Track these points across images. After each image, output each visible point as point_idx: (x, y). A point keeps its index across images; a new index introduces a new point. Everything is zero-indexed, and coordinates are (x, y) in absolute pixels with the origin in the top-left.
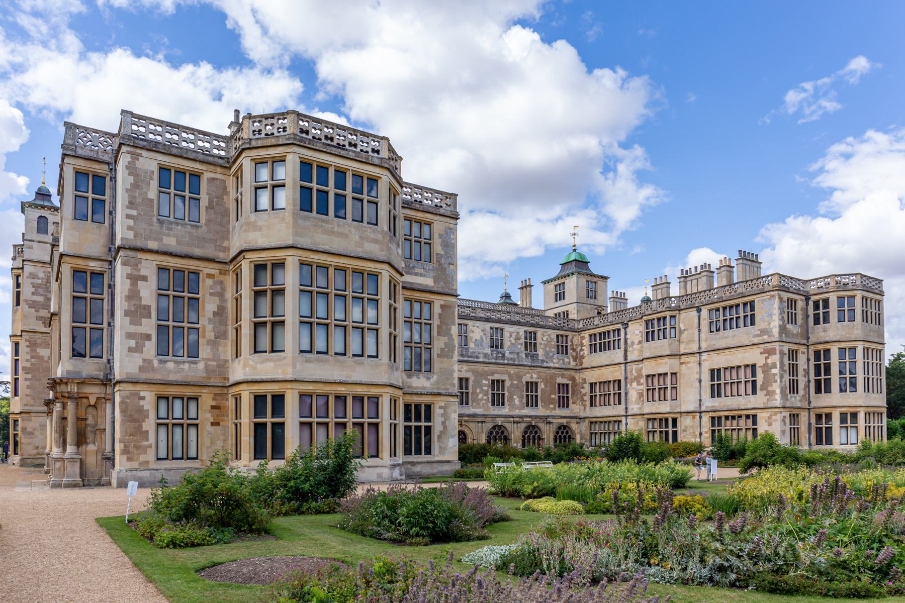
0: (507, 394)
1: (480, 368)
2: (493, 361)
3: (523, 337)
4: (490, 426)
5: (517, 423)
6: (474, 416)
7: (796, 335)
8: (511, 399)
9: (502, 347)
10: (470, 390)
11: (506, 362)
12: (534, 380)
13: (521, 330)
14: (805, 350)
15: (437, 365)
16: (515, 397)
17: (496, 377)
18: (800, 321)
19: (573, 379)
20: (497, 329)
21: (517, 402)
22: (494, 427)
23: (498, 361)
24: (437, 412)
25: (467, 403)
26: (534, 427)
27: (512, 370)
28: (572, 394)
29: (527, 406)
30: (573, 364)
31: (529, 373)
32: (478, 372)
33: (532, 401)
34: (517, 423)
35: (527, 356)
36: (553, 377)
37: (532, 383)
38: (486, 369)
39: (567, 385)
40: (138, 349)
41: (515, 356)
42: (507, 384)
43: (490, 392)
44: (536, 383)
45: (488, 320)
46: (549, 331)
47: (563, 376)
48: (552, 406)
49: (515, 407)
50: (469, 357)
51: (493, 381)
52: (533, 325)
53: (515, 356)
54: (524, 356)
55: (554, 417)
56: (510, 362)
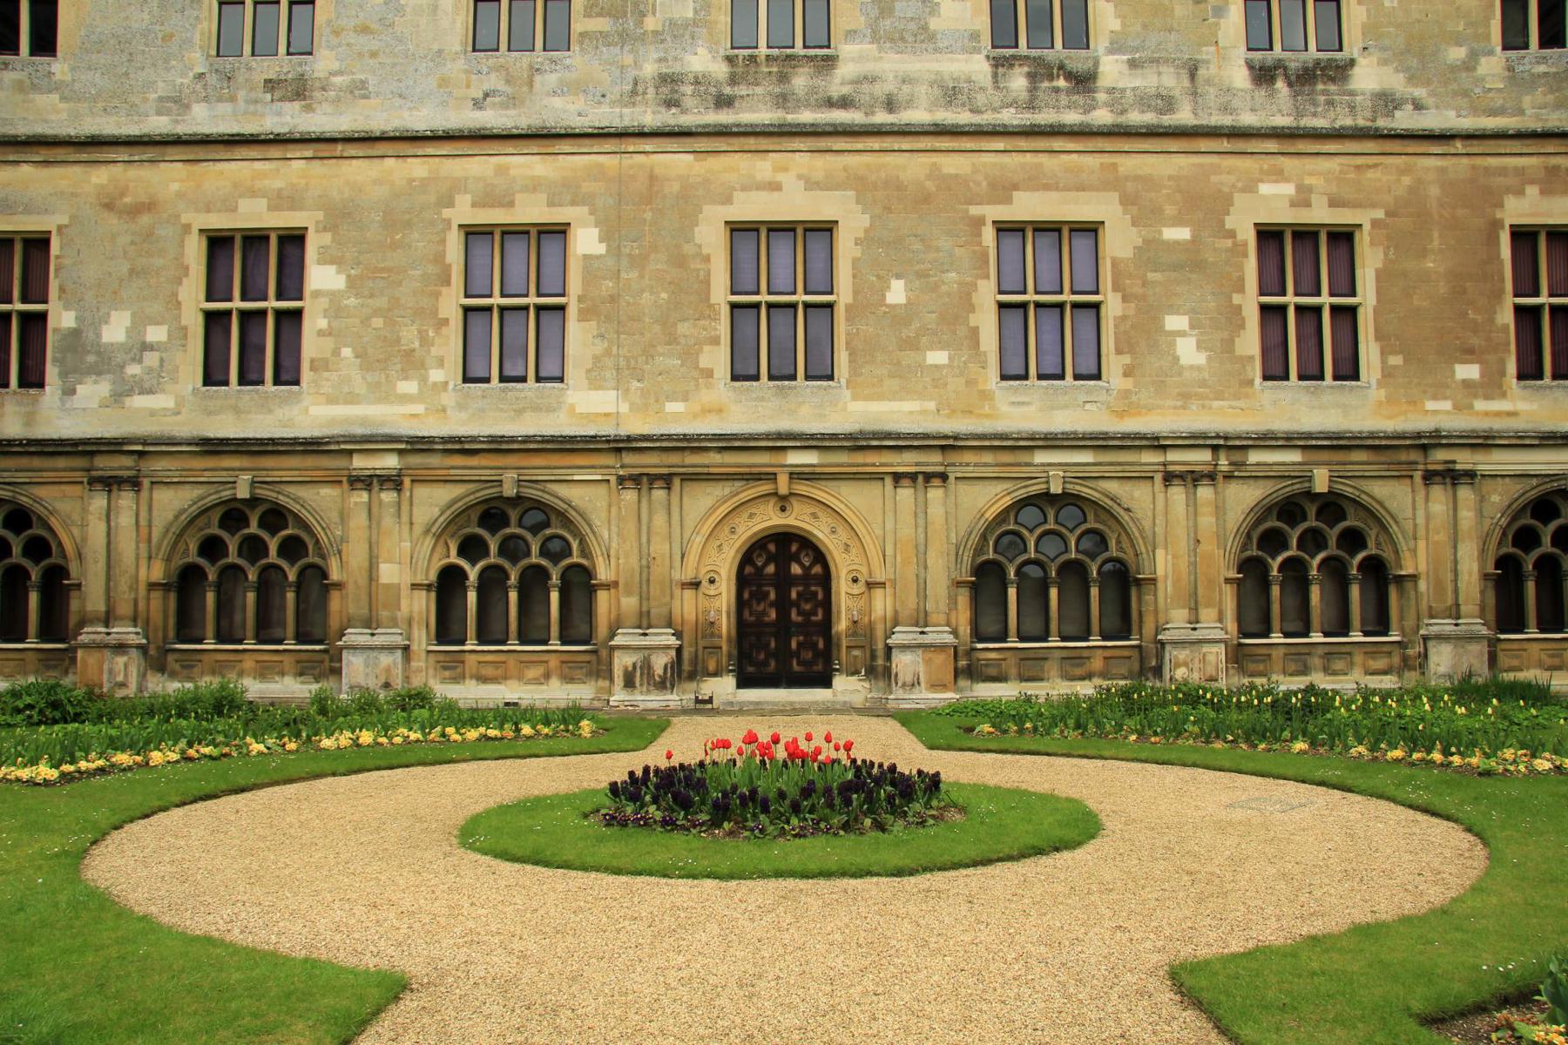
0: (1113, 306)
1: (911, 166)
2: (1009, 117)
4: (982, 499)
6: (858, 442)
8: (1145, 334)
9: (1079, 35)
10: (843, 295)
11: (1102, 117)
12: (1320, 214)
16: (1175, 322)
17: (1029, 206)
21: (1189, 352)
23: (1045, 117)
29: (1275, 372)
31: (1279, 176)
32: (896, 186)
35: (1263, 75)
37: (1306, 235)
38: (954, 165)
41: (1170, 80)
42: (1118, 243)
43: (987, 295)
44: (1343, 238)
48: (1469, 371)
50: (830, 103)
53: (1170, 80)
54: (1240, 77)
55: (1484, 442)
56: (1136, 118)
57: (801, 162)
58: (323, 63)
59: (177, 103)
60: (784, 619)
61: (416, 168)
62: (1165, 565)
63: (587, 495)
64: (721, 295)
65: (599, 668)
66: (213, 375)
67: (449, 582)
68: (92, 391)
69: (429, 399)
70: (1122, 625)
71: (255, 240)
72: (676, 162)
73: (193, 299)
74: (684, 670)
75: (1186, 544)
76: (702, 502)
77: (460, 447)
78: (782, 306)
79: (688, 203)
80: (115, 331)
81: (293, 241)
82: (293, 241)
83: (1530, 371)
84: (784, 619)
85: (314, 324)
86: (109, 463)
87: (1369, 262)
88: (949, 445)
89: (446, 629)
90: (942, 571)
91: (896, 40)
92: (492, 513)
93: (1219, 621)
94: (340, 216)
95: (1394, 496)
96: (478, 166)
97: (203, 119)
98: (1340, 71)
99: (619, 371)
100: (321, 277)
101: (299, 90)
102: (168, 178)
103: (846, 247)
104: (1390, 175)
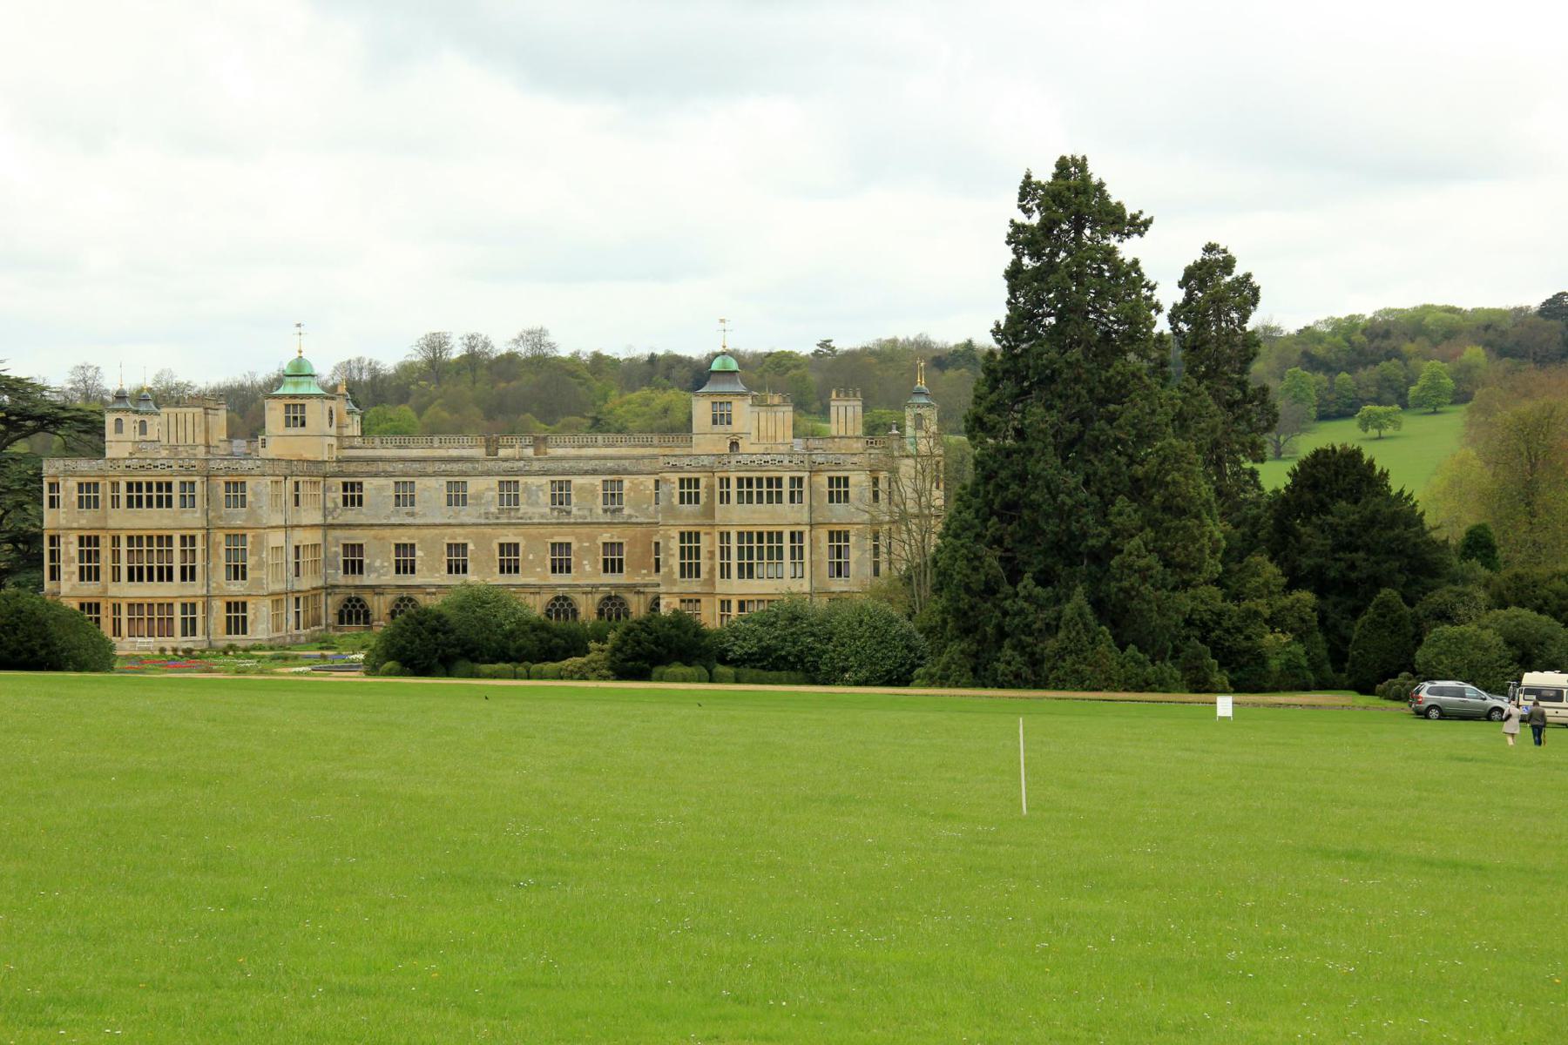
1: (533, 531)
4: (548, 597)
5: (586, 593)
8: (580, 565)
9: (569, 503)
10: (520, 557)
12: (616, 540)
13: (597, 481)
15: (249, 576)
17: (557, 539)
18: (703, 499)
20: (561, 482)
21: (588, 568)
22: (557, 599)
24: (249, 606)
27: (578, 530)
33: (613, 566)
34: (586, 593)
35: (605, 511)
40: (69, 579)
41: (586, 513)
42: (574, 547)
43: (549, 557)
45: (545, 473)
46: (642, 478)
49: (587, 572)
51: (553, 545)
52: (616, 472)
55: (646, 585)
58: (417, 508)
59: (388, 517)
62: (582, 610)
64: (498, 557)
66: (398, 571)
68: (373, 576)
71: (405, 545)
72: (488, 530)
73: (393, 558)
78: (509, 559)
80: (377, 564)
81: (413, 546)
82: (413, 546)
86: (376, 590)
88: (540, 587)
91: (532, 505)
94: (422, 541)
96: (449, 531)
97: (393, 520)
98: (620, 510)
99: (477, 572)
100: (419, 553)
101: (412, 515)
102: (387, 532)
104: (630, 531)
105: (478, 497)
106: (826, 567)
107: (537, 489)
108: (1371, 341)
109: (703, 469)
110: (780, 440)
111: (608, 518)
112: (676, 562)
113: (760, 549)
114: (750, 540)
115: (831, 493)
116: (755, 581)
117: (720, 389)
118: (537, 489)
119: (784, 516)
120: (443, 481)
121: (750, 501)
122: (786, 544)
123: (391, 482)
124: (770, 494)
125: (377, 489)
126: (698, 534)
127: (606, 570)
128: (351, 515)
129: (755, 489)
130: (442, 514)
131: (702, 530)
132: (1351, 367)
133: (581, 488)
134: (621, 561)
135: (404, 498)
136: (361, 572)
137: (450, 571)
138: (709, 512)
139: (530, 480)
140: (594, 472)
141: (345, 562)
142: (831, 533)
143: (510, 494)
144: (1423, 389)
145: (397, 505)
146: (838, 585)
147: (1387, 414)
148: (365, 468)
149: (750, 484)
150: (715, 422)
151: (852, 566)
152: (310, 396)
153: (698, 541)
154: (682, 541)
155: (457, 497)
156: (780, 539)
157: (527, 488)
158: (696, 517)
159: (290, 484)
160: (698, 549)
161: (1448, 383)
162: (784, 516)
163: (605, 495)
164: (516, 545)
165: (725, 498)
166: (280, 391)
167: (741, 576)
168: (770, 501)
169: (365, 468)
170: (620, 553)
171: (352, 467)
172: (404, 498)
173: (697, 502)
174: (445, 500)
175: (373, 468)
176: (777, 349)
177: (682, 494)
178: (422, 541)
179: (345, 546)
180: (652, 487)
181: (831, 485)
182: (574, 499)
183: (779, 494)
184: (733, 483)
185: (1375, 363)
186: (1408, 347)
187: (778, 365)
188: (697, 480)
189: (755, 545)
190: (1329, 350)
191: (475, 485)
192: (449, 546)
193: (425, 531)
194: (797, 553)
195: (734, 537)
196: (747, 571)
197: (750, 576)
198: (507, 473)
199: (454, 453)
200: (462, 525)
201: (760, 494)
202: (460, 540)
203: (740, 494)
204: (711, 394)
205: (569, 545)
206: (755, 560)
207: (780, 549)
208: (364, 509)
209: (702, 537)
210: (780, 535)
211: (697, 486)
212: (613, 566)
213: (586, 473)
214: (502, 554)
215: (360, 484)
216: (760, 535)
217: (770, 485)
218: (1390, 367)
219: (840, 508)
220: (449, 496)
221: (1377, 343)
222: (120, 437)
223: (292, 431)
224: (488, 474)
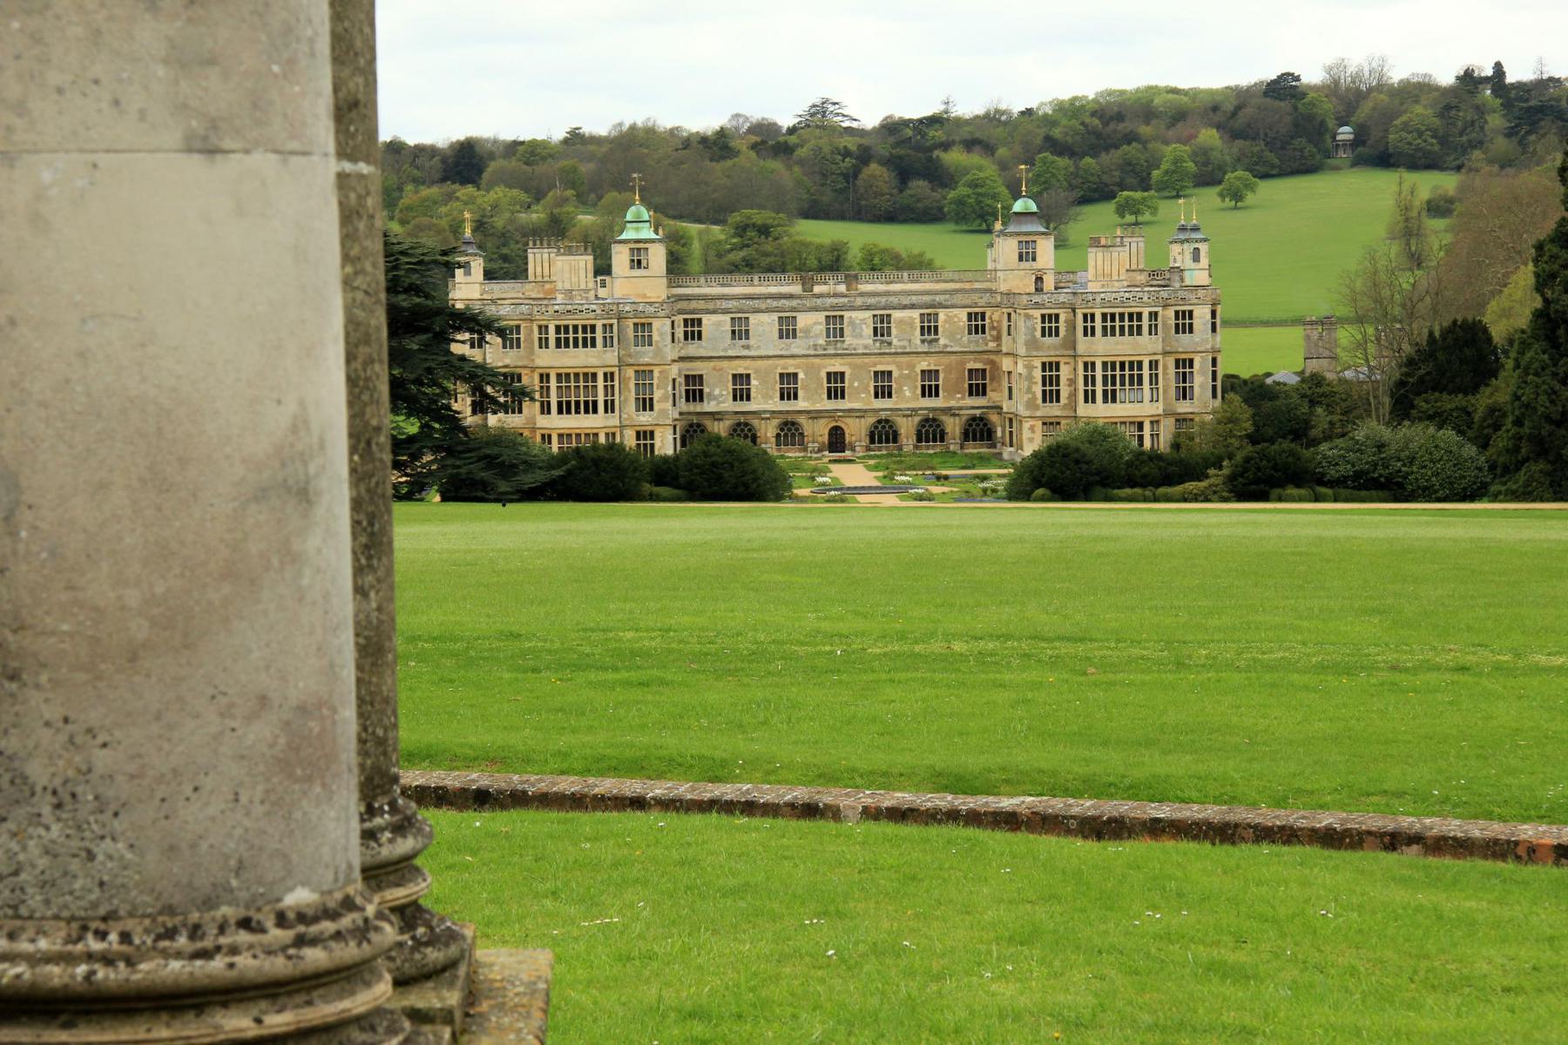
3: (918, 321)
4: (871, 420)
6: (850, 411)
7: (1056, 348)
8: (900, 390)
9: (889, 334)
13: (916, 314)
14: (1071, 360)
17: (880, 368)
18: (1062, 332)
19: (993, 363)
22: (879, 422)
25: (843, 397)
26: (934, 420)
28: (992, 379)
30: (992, 345)
33: (930, 391)
35: (923, 341)
36: (963, 363)
39: (984, 371)
41: (905, 343)
42: (895, 375)
43: (872, 384)
45: (868, 308)
46: (956, 311)
47: (975, 361)
49: (907, 397)
51: (876, 373)
53: (905, 343)
55: (961, 408)
57: (839, 360)
58: (752, 342)
60: (837, 441)
61: (770, 362)
62: (902, 431)
63: (802, 420)
64: (825, 385)
65: (805, 450)
66: (735, 399)
67: (778, 435)
68: (713, 403)
69: (776, 404)
70: (895, 441)
72: (817, 360)
73: (731, 387)
74: (820, 451)
75: (907, 428)
76: (823, 421)
77: (781, 412)
79: (819, 368)
80: (717, 392)
81: (748, 376)
82: (748, 376)
83: (971, 394)
84: (837, 441)
85: (753, 391)
87: (941, 376)
88: (865, 411)
89: (778, 444)
90: (864, 433)
92: (786, 423)
93: (912, 440)
94: (757, 371)
95: (943, 418)
96: (782, 362)
97: (730, 353)
99: (807, 399)
100: (754, 382)
101: (747, 347)
102: (725, 364)
103: (847, 377)
105: (807, 331)
106: (1173, 392)
107: (860, 322)
108: (1106, 124)
109: (1062, 305)
110: (1115, 277)
111: (925, 348)
112: (1038, 389)
113: (1123, 377)
114: (1113, 369)
115: (1177, 325)
116: (1118, 406)
117: (1025, 228)
118: (860, 322)
119: (1142, 346)
120: (775, 316)
121: (1113, 334)
122: (1146, 372)
123: (727, 318)
124: (1131, 327)
125: (715, 325)
126: (1058, 364)
127: (923, 395)
128: (693, 349)
129: (1117, 324)
130: (774, 346)
131: (1062, 360)
132: (1094, 151)
133: (901, 321)
134: (937, 387)
135: (740, 332)
136: (701, 400)
137: (782, 398)
138: (1071, 344)
139: (854, 314)
140: (913, 307)
141: (687, 391)
142: (1177, 361)
143: (835, 327)
144: (1166, 172)
145: (733, 338)
146: (1184, 407)
147: (1144, 199)
148: (701, 305)
149: (1113, 320)
150: (1021, 259)
151: (1197, 390)
152: (652, 241)
153: (1058, 370)
154: (1044, 370)
155: (788, 331)
156: (1140, 368)
157: (852, 323)
158: (1056, 348)
159: (668, 322)
160: (1058, 377)
161: (1190, 166)
162: (1142, 346)
163: (922, 328)
164: (843, 374)
165: (1089, 332)
166: (623, 237)
167: (1105, 401)
168: (1131, 334)
169: (701, 305)
170: (937, 379)
171: (694, 305)
172: (740, 332)
173: (1057, 335)
174: (777, 335)
175: (711, 306)
176: (525, 136)
177: (1043, 329)
178: (757, 371)
179: (687, 377)
180: (965, 318)
181: (1177, 318)
182: (894, 331)
183: (1140, 327)
184: (1098, 318)
185: (1117, 147)
186: (1144, 130)
187: (533, 153)
188: (1057, 316)
189: (1118, 372)
190: (1066, 134)
191: (804, 320)
192: (781, 375)
193: (760, 363)
194: (1154, 379)
195: (1099, 367)
196: (1110, 397)
197: (1114, 400)
198: (833, 308)
199: (773, 290)
200: (792, 356)
201: (1122, 328)
202: (791, 370)
203: (1105, 328)
204: (1018, 234)
205: (890, 373)
206: (1118, 387)
207: (1140, 377)
208: (703, 343)
209: (1062, 367)
210: (1140, 364)
211: (1057, 321)
212: (930, 391)
213: (905, 307)
214: (829, 381)
215: (700, 320)
216: (1122, 365)
217: (1131, 319)
218: (1131, 150)
219: (1185, 338)
220: (781, 331)
221: (1112, 126)
222: (468, 279)
223: (637, 272)
224: (816, 309)
